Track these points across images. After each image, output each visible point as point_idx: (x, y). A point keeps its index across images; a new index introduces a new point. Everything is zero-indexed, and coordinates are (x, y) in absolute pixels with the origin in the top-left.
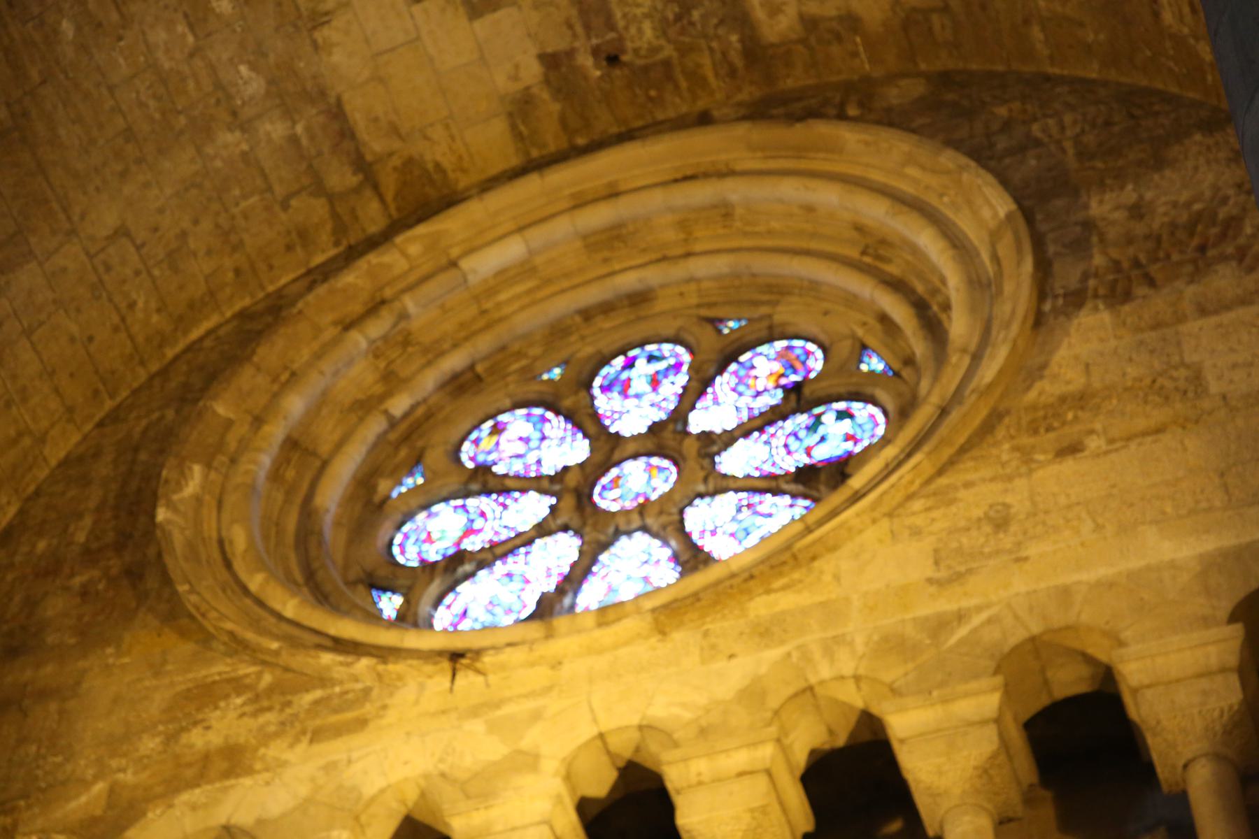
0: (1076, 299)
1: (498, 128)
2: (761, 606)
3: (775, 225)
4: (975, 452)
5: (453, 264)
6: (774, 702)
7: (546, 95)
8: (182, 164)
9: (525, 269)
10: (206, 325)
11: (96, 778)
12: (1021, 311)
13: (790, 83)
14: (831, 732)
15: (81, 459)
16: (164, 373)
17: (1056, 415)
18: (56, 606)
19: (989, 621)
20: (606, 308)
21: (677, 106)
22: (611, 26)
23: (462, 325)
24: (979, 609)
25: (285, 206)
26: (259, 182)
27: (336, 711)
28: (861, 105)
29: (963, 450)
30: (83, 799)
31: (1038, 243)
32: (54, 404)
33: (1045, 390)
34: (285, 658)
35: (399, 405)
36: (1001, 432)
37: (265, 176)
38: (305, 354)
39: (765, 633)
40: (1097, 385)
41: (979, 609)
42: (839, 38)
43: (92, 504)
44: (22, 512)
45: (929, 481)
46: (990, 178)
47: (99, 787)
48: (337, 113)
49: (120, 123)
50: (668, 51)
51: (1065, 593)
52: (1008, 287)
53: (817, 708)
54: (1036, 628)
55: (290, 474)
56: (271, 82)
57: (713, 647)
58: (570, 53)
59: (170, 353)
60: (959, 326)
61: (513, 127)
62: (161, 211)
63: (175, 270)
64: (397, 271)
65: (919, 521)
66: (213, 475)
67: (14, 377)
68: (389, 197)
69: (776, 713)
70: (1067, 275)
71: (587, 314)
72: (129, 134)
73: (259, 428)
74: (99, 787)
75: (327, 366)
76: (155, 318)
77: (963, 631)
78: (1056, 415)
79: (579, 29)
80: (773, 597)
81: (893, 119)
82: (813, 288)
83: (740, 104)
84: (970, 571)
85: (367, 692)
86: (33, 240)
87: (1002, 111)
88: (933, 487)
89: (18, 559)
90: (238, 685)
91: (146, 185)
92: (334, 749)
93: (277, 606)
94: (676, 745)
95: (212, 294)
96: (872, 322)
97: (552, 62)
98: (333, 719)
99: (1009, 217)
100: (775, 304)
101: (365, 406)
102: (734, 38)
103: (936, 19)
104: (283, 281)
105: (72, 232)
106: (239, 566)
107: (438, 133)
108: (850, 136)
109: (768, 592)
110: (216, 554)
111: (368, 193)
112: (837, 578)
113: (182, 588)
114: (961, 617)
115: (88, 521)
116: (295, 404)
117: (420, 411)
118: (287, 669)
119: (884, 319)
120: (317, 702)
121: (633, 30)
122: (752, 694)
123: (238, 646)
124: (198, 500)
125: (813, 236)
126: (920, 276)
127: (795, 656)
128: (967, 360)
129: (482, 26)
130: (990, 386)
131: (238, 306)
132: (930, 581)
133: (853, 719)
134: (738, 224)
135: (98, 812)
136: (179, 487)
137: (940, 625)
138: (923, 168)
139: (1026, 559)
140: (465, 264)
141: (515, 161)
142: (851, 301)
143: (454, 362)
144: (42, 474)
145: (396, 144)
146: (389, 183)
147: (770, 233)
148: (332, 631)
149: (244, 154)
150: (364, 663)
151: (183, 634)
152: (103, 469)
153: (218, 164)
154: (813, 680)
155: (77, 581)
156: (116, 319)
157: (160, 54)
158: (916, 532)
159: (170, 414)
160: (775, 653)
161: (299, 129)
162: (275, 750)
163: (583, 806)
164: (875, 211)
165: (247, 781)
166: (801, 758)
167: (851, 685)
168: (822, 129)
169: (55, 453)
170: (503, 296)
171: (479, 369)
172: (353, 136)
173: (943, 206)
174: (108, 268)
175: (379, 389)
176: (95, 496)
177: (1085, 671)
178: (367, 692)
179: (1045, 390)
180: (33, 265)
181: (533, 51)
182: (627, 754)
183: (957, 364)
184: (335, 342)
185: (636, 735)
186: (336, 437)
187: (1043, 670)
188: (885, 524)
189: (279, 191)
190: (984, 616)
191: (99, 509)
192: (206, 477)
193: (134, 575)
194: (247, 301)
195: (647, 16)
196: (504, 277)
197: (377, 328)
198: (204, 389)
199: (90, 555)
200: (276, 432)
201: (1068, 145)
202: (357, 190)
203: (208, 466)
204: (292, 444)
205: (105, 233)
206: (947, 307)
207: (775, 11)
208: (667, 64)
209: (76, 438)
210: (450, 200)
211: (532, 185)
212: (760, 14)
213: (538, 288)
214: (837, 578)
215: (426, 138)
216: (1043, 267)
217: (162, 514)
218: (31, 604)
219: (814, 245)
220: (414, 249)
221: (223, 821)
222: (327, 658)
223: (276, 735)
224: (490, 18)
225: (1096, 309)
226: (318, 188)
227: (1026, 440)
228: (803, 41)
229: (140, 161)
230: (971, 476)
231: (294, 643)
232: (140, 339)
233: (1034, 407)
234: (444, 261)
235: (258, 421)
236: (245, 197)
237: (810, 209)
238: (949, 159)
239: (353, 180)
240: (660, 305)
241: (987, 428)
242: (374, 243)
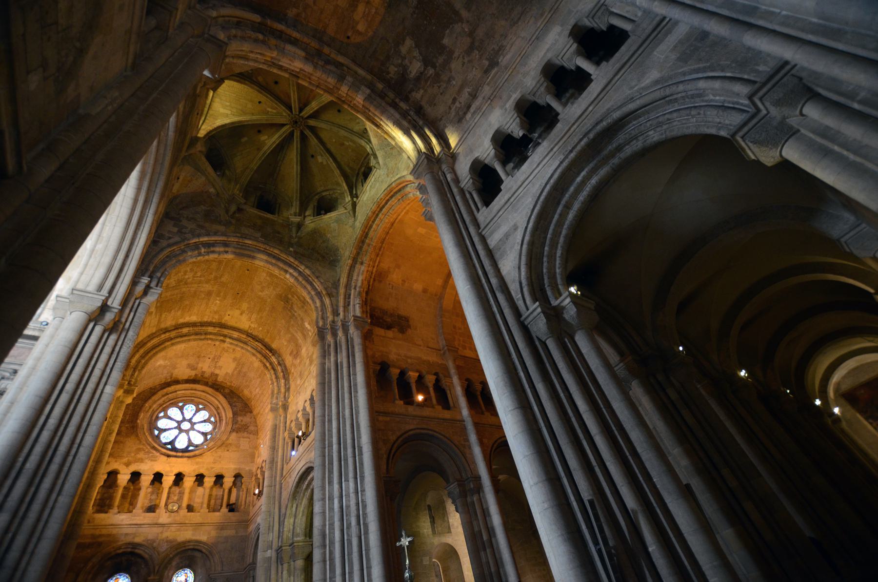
33: (228, 442)
39: (197, 463)
74: (127, 459)
92: (153, 463)
123: (144, 444)
137: (212, 468)
155: (127, 425)
158: (213, 456)
162: (147, 461)
217: (138, 421)
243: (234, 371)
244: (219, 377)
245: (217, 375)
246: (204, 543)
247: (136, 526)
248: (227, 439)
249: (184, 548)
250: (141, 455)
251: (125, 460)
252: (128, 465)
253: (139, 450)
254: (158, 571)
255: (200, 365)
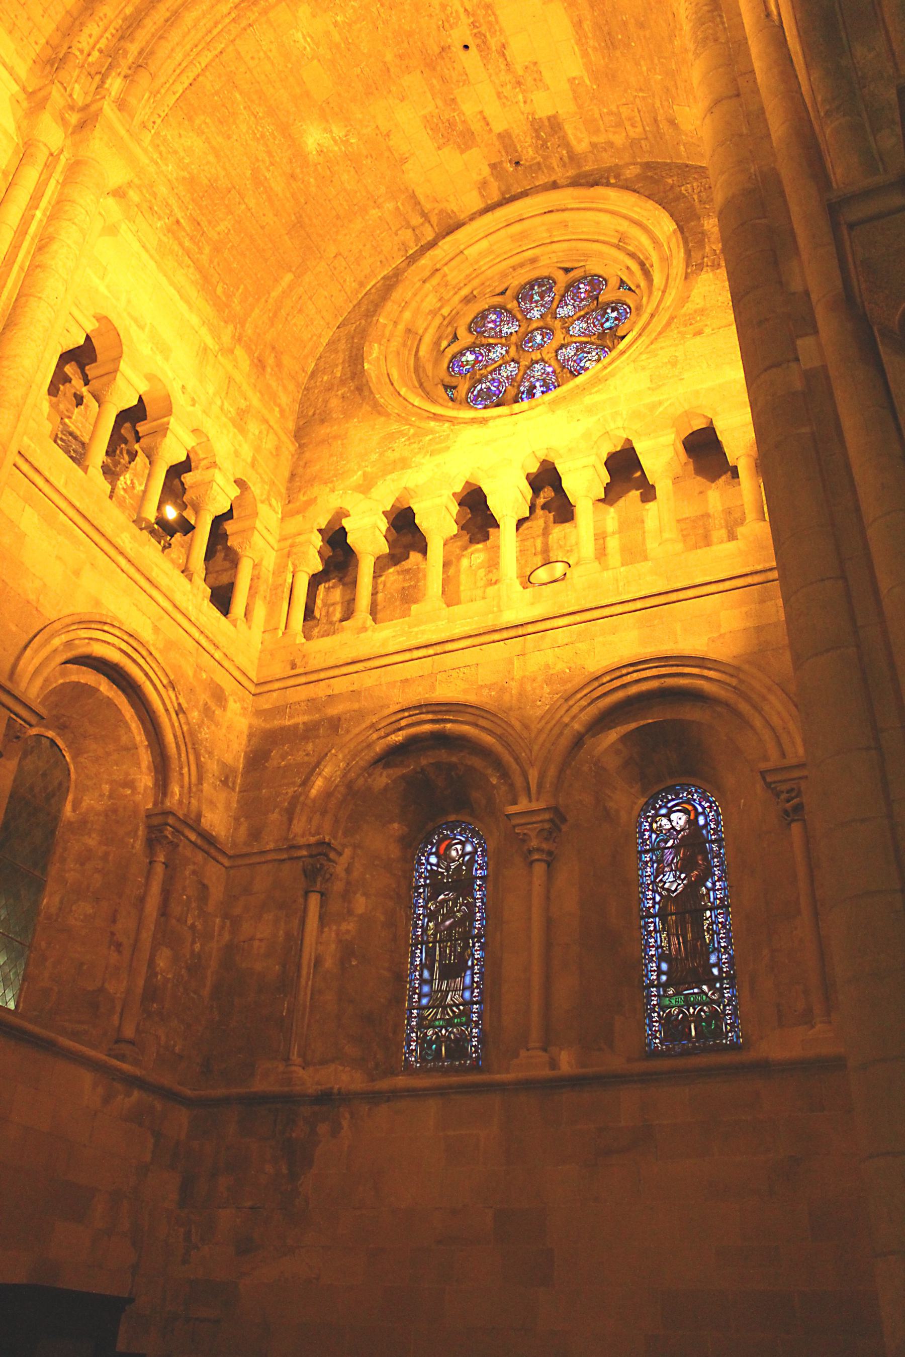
0: (700, 267)
1: (475, 193)
2: (588, 400)
3: (585, 230)
4: (664, 334)
5: (462, 252)
6: (594, 438)
7: (492, 180)
8: (358, 224)
9: (490, 251)
10: (372, 283)
11: (358, 470)
12: (679, 274)
13: (587, 168)
14: (615, 446)
15: (333, 342)
16: (359, 303)
17: (694, 318)
18: (334, 403)
19: (671, 405)
20: (521, 265)
21: (542, 180)
22: (517, 151)
23: (467, 276)
24: (667, 400)
25: (396, 234)
26: (386, 226)
27: (437, 443)
28: (616, 177)
29: (660, 333)
30: (355, 478)
31: (686, 242)
32: (322, 323)
34: (417, 423)
35: (445, 311)
36: (673, 326)
37: (388, 224)
38: (410, 294)
39: (590, 410)
40: (708, 305)
41: (667, 400)
42: (605, 150)
43: (341, 361)
44: (316, 365)
45: (647, 347)
46: (667, 214)
47: (360, 473)
48: (413, 196)
49: (334, 213)
50: (539, 159)
51: (697, 393)
52: (675, 262)
53: (610, 439)
54: (687, 408)
55: (409, 343)
56: (387, 188)
57: (571, 417)
58: (501, 162)
59: (360, 296)
60: (658, 279)
61: (480, 193)
62: (352, 243)
63: (359, 265)
64: (440, 257)
65: (643, 363)
66: (382, 347)
67: (307, 315)
68: (435, 225)
69: (596, 442)
70: (696, 256)
71: (514, 268)
72: (338, 217)
73: (396, 327)
74: (360, 473)
75: (418, 298)
76: (353, 284)
77: (661, 409)
78: (694, 318)
79: (503, 153)
80: (592, 396)
81: (627, 187)
82: (601, 254)
83: (568, 178)
84: (663, 385)
85: (448, 435)
86: (308, 263)
87: (670, 181)
88: (649, 349)
89: (318, 384)
90: (402, 434)
91: (345, 235)
92: (438, 459)
93: (411, 401)
94: (561, 456)
95: (372, 271)
96: (624, 269)
97: (493, 166)
98: (437, 447)
99: (674, 231)
100: (586, 261)
101: (434, 313)
102: (564, 152)
103: (642, 142)
104: (398, 262)
105: (321, 257)
106: (395, 384)
107: (452, 198)
108: (612, 194)
109: (591, 394)
110: (387, 380)
111: (427, 225)
112: (615, 388)
113: (377, 396)
114: (660, 403)
115: (340, 368)
116: (407, 315)
117: (454, 312)
118: (419, 427)
119: (628, 268)
120: (430, 440)
121: (524, 152)
122: (587, 435)
124: (378, 358)
125: (599, 234)
126: (641, 251)
127: (602, 420)
128: (660, 293)
129: (466, 156)
130: (668, 307)
131: (382, 275)
132: (649, 388)
133: (623, 441)
134: (570, 229)
135: (361, 482)
136: (371, 354)
137: (653, 407)
138: (641, 208)
139: (683, 379)
140: (466, 252)
141: (482, 206)
142: (615, 260)
143: (465, 292)
144: (321, 349)
145: (436, 205)
146: (434, 220)
147: (583, 233)
148: (433, 411)
149: (380, 217)
150: (447, 425)
151: (380, 413)
152: (342, 345)
153: (370, 222)
154: (608, 429)
155: (340, 393)
156: (340, 287)
157: (346, 185)
158: (643, 368)
159: (363, 322)
160: (595, 418)
161: (399, 204)
162: (418, 459)
163: (528, 476)
164: (624, 226)
165: (410, 471)
166: (605, 457)
167: (622, 431)
168: (600, 190)
169: (324, 341)
170: (482, 263)
171: (475, 293)
172: (419, 203)
173: (648, 224)
174: (335, 269)
175: (439, 305)
176: (341, 356)
177: (704, 420)
178: (448, 435)
179: (689, 307)
180: (309, 272)
181: (487, 163)
182: (543, 458)
183: (657, 294)
184: (420, 289)
185: (546, 451)
186: (425, 325)
187: (689, 422)
188: (632, 365)
189: (394, 229)
190: (669, 402)
191: (343, 362)
192: (379, 348)
193: (359, 389)
194: (386, 272)
195: (529, 146)
196: (482, 255)
197: (435, 281)
198: (375, 311)
199: (343, 382)
200: (401, 327)
201: (696, 197)
202: (422, 224)
203: (380, 344)
204: (408, 331)
205: (333, 255)
206: (652, 266)
207: (580, 141)
208: (539, 163)
209: (331, 333)
210: (459, 225)
211: (489, 217)
212: (574, 142)
213: (494, 259)
214: (615, 388)
215: (447, 201)
216: (688, 253)
217: (366, 366)
218: (326, 402)
219: (602, 238)
220: (446, 247)
221: (404, 485)
222: (432, 424)
223: (418, 453)
224: (469, 152)
225: (707, 272)
226: (408, 226)
227: (683, 329)
228: (592, 152)
229: (342, 226)
230: (663, 345)
231: (421, 418)
232: (349, 293)
233: (685, 315)
234: (458, 251)
235: (396, 323)
236: (382, 233)
237: (598, 223)
238: (650, 204)
239: (421, 220)
240: (541, 264)
241: (668, 324)
242: (432, 244)
243: (585, 54)
244: (569, 129)
245: (554, 124)
246: (700, 662)
247: (431, 651)
248: (684, 299)
249: (620, 695)
250: (400, 448)
251: (356, 478)
252: (365, 487)
253: (391, 437)
254: (540, 785)
255: (469, 109)
